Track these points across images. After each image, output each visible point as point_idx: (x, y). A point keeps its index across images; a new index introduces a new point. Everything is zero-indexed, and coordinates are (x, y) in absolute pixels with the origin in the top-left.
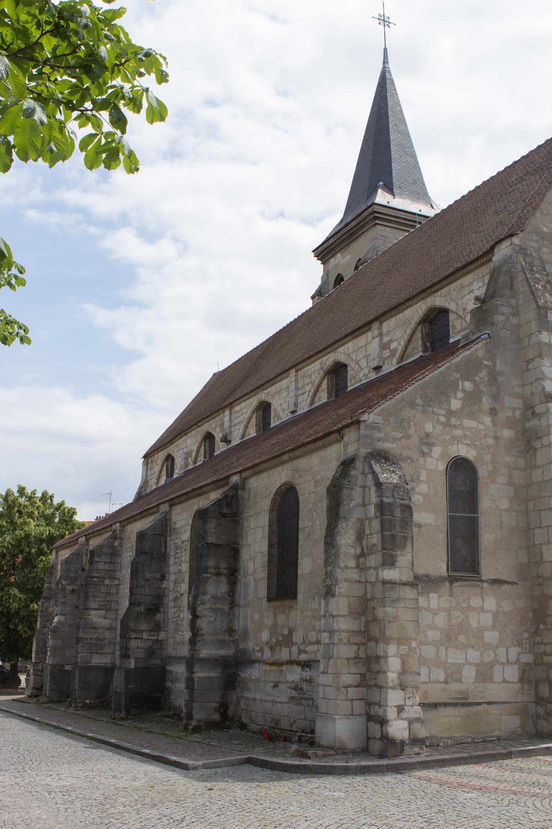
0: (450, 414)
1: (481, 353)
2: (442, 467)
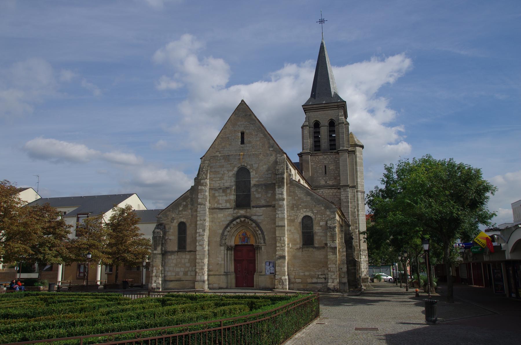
0: (179, 211)
1: (188, 194)
2: (177, 225)
